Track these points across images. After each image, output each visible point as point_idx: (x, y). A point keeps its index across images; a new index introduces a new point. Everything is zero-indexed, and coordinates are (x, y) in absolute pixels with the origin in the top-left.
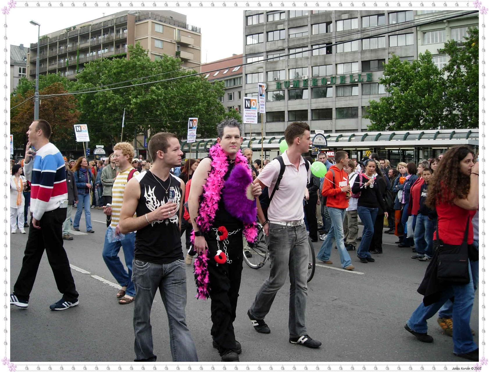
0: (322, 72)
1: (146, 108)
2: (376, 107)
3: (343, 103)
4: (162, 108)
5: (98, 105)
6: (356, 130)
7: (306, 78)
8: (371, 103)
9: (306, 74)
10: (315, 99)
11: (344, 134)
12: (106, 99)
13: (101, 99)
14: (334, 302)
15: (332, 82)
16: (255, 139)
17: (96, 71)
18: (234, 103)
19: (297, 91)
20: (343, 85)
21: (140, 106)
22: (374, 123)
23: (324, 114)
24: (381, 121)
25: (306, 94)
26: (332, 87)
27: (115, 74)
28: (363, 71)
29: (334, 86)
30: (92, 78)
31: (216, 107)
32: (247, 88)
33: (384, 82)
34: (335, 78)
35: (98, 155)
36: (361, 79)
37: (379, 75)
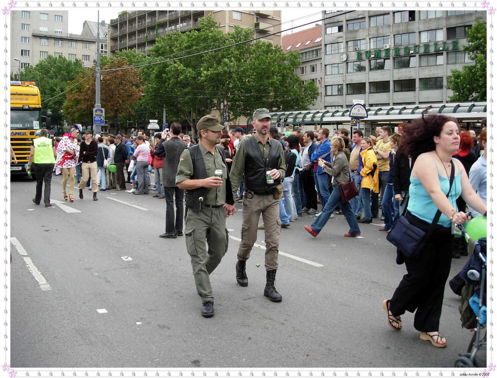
0: (404, 40)
1: (217, 81)
2: (457, 77)
3: (427, 73)
4: (234, 81)
5: (169, 79)
7: (388, 47)
8: (453, 72)
9: (389, 44)
10: (396, 71)
12: (178, 73)
13: (172, 73)
15: (415, 51)
16: (328, 112)
17: (168, 45)
18: (307, 76)
19: (378, 61)
20: (427, 54)
22: (457, 94)
23: (407, 85)
25: (389, 64)
26: (415, 56)
28: (448, 38)
29: (417, 56)
32: (327, 59)
34: (419, 46)
35: (152, 130)
36: (446, 47)
37: (464, 43)
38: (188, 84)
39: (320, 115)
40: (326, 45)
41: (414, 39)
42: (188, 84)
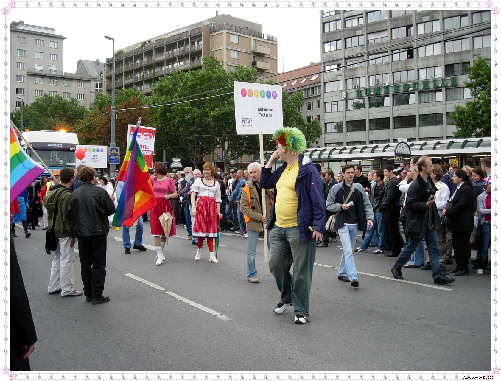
0: (403, 77)
2: (461, 112)
3: (426, 110)
5: (174, 118)
6: (441, 138)
7: (387, 84)
8: (456, 108)
9: (387, 80)
10: (396, 107)
11: (428, 142)
12: (183, 112)
14: (419, 321)
15: (414, 87)
16: (335, 149)
18: (313, 113)
19: (378, 98)
20: (426, 91)
21: (217, 119)
22: (460, 129)
23: (407, 122)
24: (467, 127)
25: (388, 101)
26: (414, 93)
27: (190, 86)
28: (446, 75)
29: (417, 92)
30: (168, 92)
31: (294, 117)
32: (326, 97)
33: (469, 86)
36: (445, 84)
37: (464, 79)
38: (194, 123)
39: (328, 152)
40: (325, 83)
41: (412, 76)
42: (194, 123)
